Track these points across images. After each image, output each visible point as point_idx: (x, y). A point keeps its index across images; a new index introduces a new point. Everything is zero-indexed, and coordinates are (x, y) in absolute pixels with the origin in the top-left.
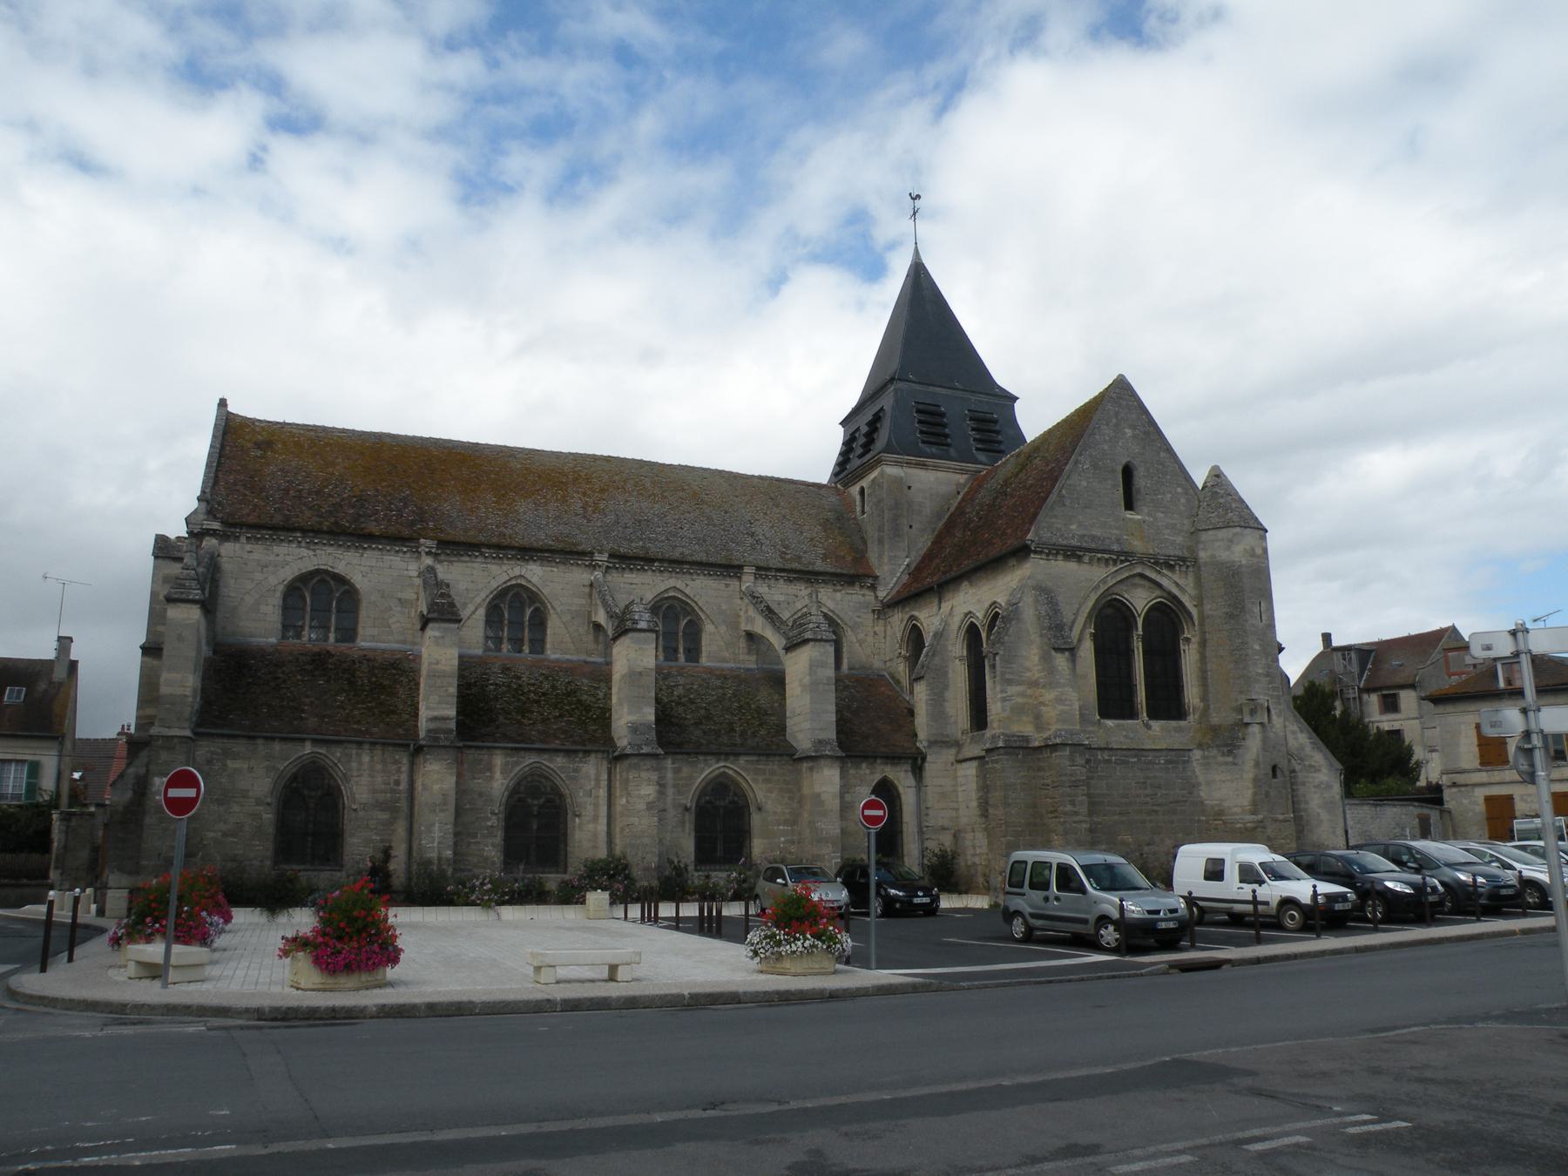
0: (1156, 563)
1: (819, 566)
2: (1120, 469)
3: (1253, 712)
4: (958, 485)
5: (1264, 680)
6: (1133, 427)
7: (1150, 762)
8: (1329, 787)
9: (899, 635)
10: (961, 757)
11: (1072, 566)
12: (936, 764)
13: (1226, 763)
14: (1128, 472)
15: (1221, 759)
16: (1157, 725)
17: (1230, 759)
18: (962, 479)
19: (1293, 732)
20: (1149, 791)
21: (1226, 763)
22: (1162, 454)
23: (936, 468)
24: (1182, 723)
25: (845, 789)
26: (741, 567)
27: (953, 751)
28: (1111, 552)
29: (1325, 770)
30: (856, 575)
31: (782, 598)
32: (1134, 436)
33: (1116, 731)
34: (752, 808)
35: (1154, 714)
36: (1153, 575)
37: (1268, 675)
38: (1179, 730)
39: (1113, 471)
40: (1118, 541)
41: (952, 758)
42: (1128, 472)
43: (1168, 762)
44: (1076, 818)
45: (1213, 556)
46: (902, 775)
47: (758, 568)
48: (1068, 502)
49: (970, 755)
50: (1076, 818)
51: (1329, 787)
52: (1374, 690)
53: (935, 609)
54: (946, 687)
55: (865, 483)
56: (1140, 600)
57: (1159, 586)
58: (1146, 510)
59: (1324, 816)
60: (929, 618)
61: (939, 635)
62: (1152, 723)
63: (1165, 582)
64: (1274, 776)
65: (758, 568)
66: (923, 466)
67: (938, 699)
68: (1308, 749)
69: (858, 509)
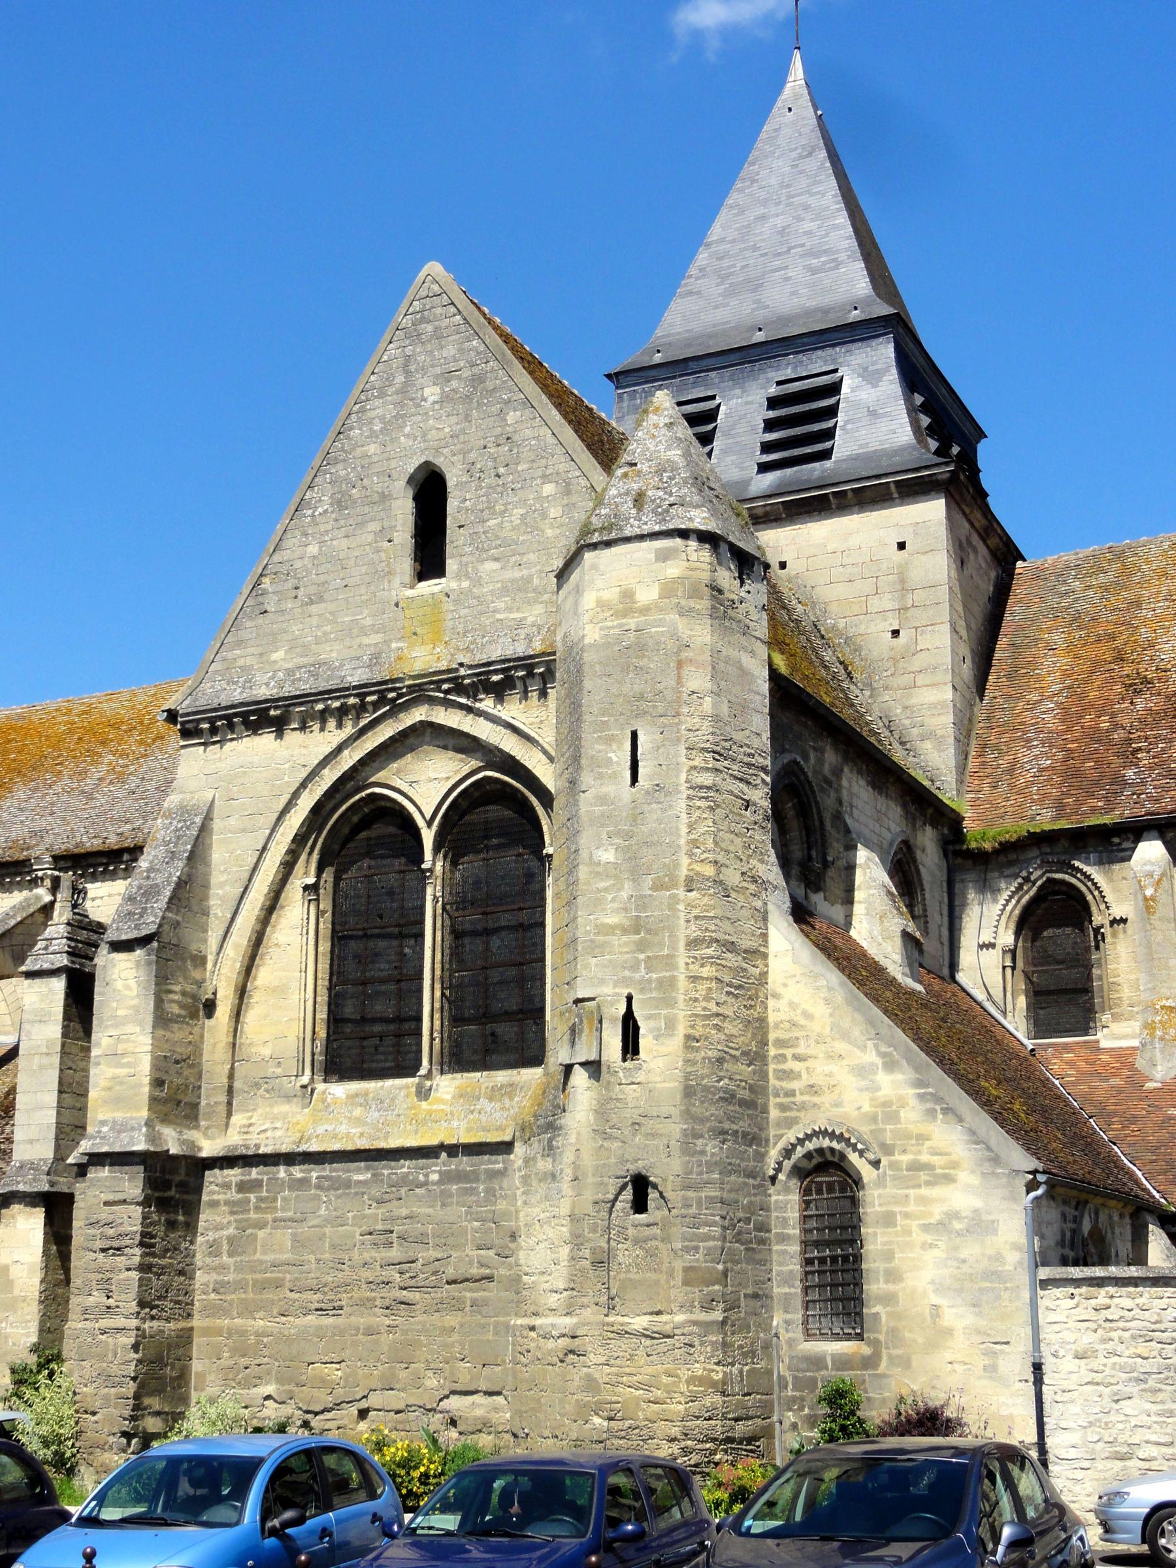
11: (266, 740)
14: (430, 491)
19: (862, 1071)
20: (395, 1253)
29: (965, 1177)
32: (445, 399)
33: (356, 1112)
35: (460, 1057)
42: (430, 491)
43: (446, 1178)
44: (104, 1323)
50: (104, 1323)
51: (979, 1226)
56: (426, 785)
58: (451, 565)
59: (957, 1317)
64: (640, 1205)
68: (912, 1115)
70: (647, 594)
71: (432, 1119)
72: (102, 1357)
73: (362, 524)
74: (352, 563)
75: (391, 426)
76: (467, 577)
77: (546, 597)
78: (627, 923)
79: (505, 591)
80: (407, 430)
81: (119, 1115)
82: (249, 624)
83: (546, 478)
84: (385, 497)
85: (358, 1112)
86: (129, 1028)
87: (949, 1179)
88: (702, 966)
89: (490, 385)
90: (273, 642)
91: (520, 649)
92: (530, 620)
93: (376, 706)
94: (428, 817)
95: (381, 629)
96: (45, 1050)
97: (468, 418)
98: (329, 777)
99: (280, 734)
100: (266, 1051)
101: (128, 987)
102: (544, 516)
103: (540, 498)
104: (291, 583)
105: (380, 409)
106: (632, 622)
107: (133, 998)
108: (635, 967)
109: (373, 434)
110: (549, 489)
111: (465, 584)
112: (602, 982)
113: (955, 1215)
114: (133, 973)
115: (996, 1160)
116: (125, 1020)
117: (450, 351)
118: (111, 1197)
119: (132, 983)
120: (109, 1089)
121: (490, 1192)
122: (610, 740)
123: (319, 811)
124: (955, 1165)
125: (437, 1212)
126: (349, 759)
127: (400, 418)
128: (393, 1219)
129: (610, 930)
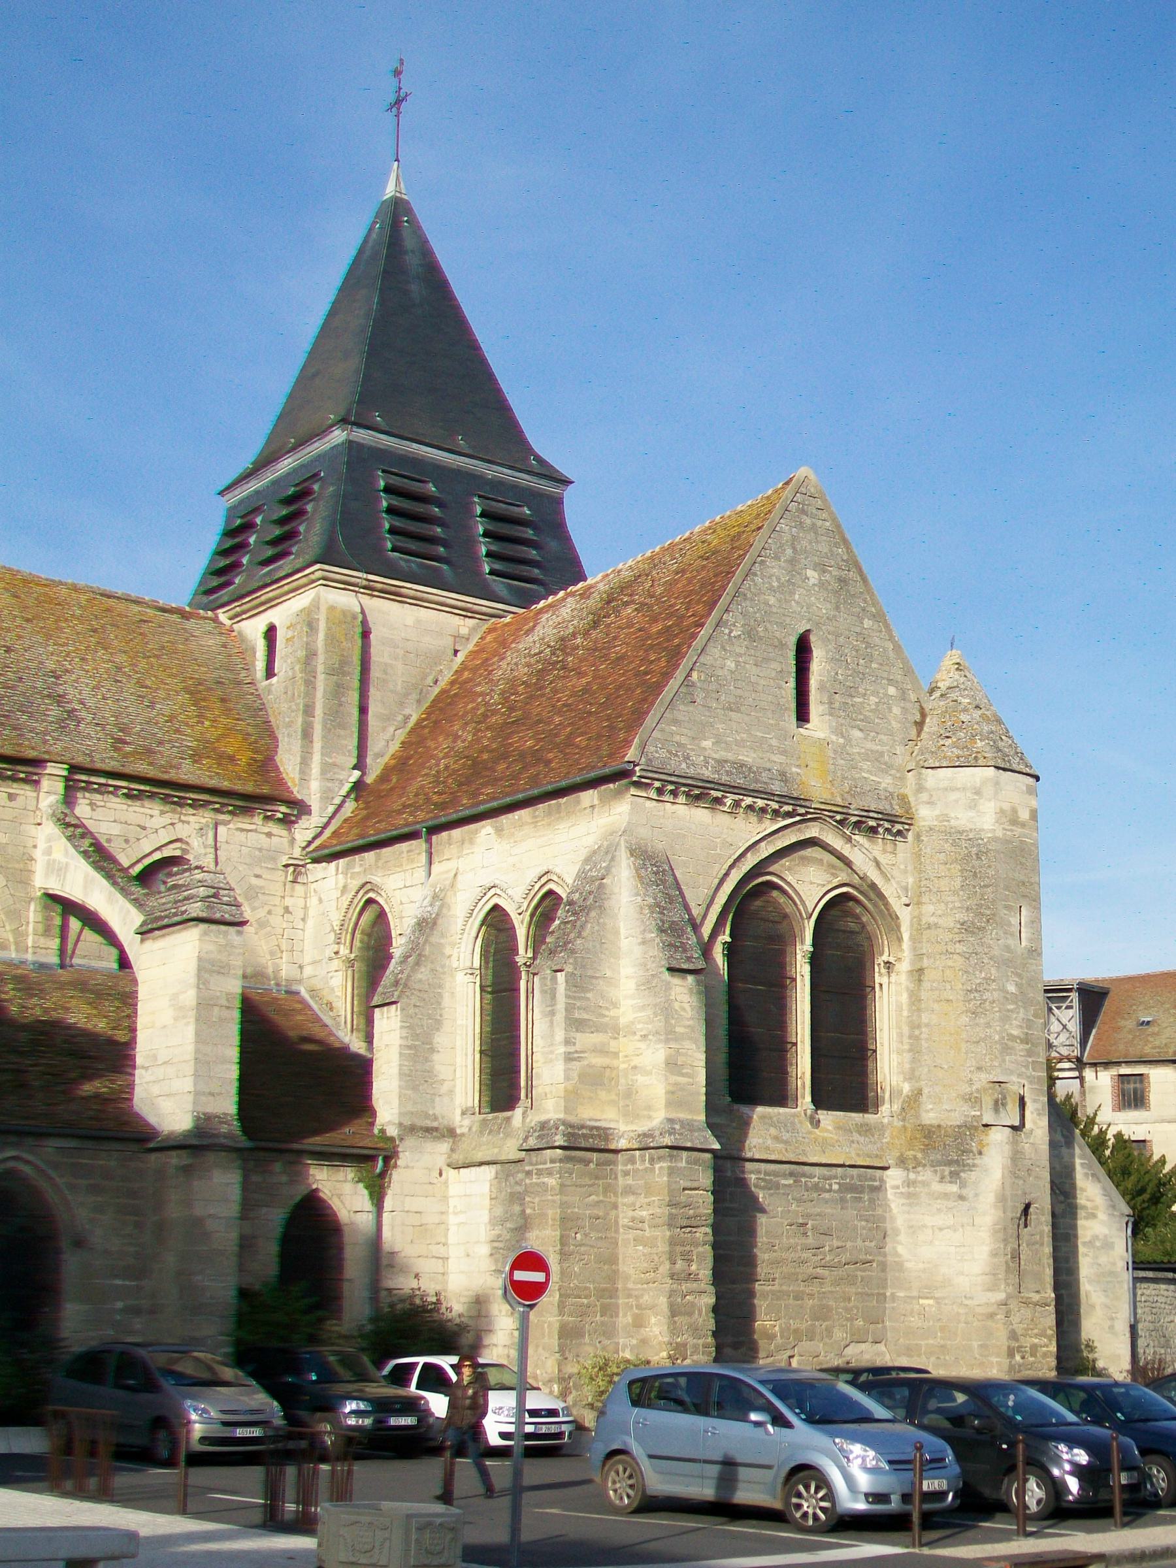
1: (187, 772)
2: (792, 641)
3: (998, 1105)
4: (457, 637)
5: (1020, 1047)
6: (821, 568)
7: (816, 1188)
8: (1108, 1245)
9: (336, 918)
10: (459, 1157)
11: (700, 815)
12: (414, 1167)
13: (946, 1196)
15: (937, 1187)
16: (829, 1119)
17: (954, 1188)
18: (465, 626)
20: (810, 1241)
21: (946, 1196)
22: (867, 623)
23: (418, 601)
24: (869, 1117)
25: (248, 1207)
26: (38, 763)
27: (444, 1147)
28: (769, 795)
29: (1102, 1216)
30: (260, 795)
31: (115, 829)
32: (822, 584)
34: (65, 1243)
35: (821, 1100)
36: (836, 842)
37: (1026, 1040)
38: (865, 1130)
39: (783, 645)
40: (784, 776)
41: (441, 1161)
46: (348, 1188)
47: (74, 768)
48: (700, 696)
49: (479, 1156)
51: (1108, 1245)
52: (1107, 1065)
53: (421, 873)
54: (438, 1024)
55: (281, 615)
57: (848, 863)
60: (401, 882)
61: (426, 925)
62: (823, 1115)
65: (74, 768)
66: (395, 595)
67: (420, 1048)
69: (260, 665)
70: (1024, 815)
71: (824, 1145)
72: (690, 1314)
73: (767, 660)
74: (760, 688)
75: (787, 588)
76: (843, 737)
77: (893, 772)
78: (1022, 1036)
80: (797, 597)
82: (682, 707)
83: (891, 682)
85: (773, 1131)
87: (1094, 1216)
92: (883, 785)
93: (789, 815)
94: (810, 911)
96: (225, 1003)
99: (760, 820)
101: (684, 1009)
103: (886, 695)
105: (776, 570)
106: (1018, 830)
107: (688, 1019)
108: (1026, 1067)
109: (771, 588)
110: (892, 691)
111: (841, 741)
112: (1012, 1072)
113: (1096, 1237)
114: (686, 998)
115: (1113, 1207)
118: (689, 1184)
119: (687, 1006)
120: (673, 1093)
121: (872, 1201)
124: (1096, 1208)
126: (766, 850)
128: (809, 1216)
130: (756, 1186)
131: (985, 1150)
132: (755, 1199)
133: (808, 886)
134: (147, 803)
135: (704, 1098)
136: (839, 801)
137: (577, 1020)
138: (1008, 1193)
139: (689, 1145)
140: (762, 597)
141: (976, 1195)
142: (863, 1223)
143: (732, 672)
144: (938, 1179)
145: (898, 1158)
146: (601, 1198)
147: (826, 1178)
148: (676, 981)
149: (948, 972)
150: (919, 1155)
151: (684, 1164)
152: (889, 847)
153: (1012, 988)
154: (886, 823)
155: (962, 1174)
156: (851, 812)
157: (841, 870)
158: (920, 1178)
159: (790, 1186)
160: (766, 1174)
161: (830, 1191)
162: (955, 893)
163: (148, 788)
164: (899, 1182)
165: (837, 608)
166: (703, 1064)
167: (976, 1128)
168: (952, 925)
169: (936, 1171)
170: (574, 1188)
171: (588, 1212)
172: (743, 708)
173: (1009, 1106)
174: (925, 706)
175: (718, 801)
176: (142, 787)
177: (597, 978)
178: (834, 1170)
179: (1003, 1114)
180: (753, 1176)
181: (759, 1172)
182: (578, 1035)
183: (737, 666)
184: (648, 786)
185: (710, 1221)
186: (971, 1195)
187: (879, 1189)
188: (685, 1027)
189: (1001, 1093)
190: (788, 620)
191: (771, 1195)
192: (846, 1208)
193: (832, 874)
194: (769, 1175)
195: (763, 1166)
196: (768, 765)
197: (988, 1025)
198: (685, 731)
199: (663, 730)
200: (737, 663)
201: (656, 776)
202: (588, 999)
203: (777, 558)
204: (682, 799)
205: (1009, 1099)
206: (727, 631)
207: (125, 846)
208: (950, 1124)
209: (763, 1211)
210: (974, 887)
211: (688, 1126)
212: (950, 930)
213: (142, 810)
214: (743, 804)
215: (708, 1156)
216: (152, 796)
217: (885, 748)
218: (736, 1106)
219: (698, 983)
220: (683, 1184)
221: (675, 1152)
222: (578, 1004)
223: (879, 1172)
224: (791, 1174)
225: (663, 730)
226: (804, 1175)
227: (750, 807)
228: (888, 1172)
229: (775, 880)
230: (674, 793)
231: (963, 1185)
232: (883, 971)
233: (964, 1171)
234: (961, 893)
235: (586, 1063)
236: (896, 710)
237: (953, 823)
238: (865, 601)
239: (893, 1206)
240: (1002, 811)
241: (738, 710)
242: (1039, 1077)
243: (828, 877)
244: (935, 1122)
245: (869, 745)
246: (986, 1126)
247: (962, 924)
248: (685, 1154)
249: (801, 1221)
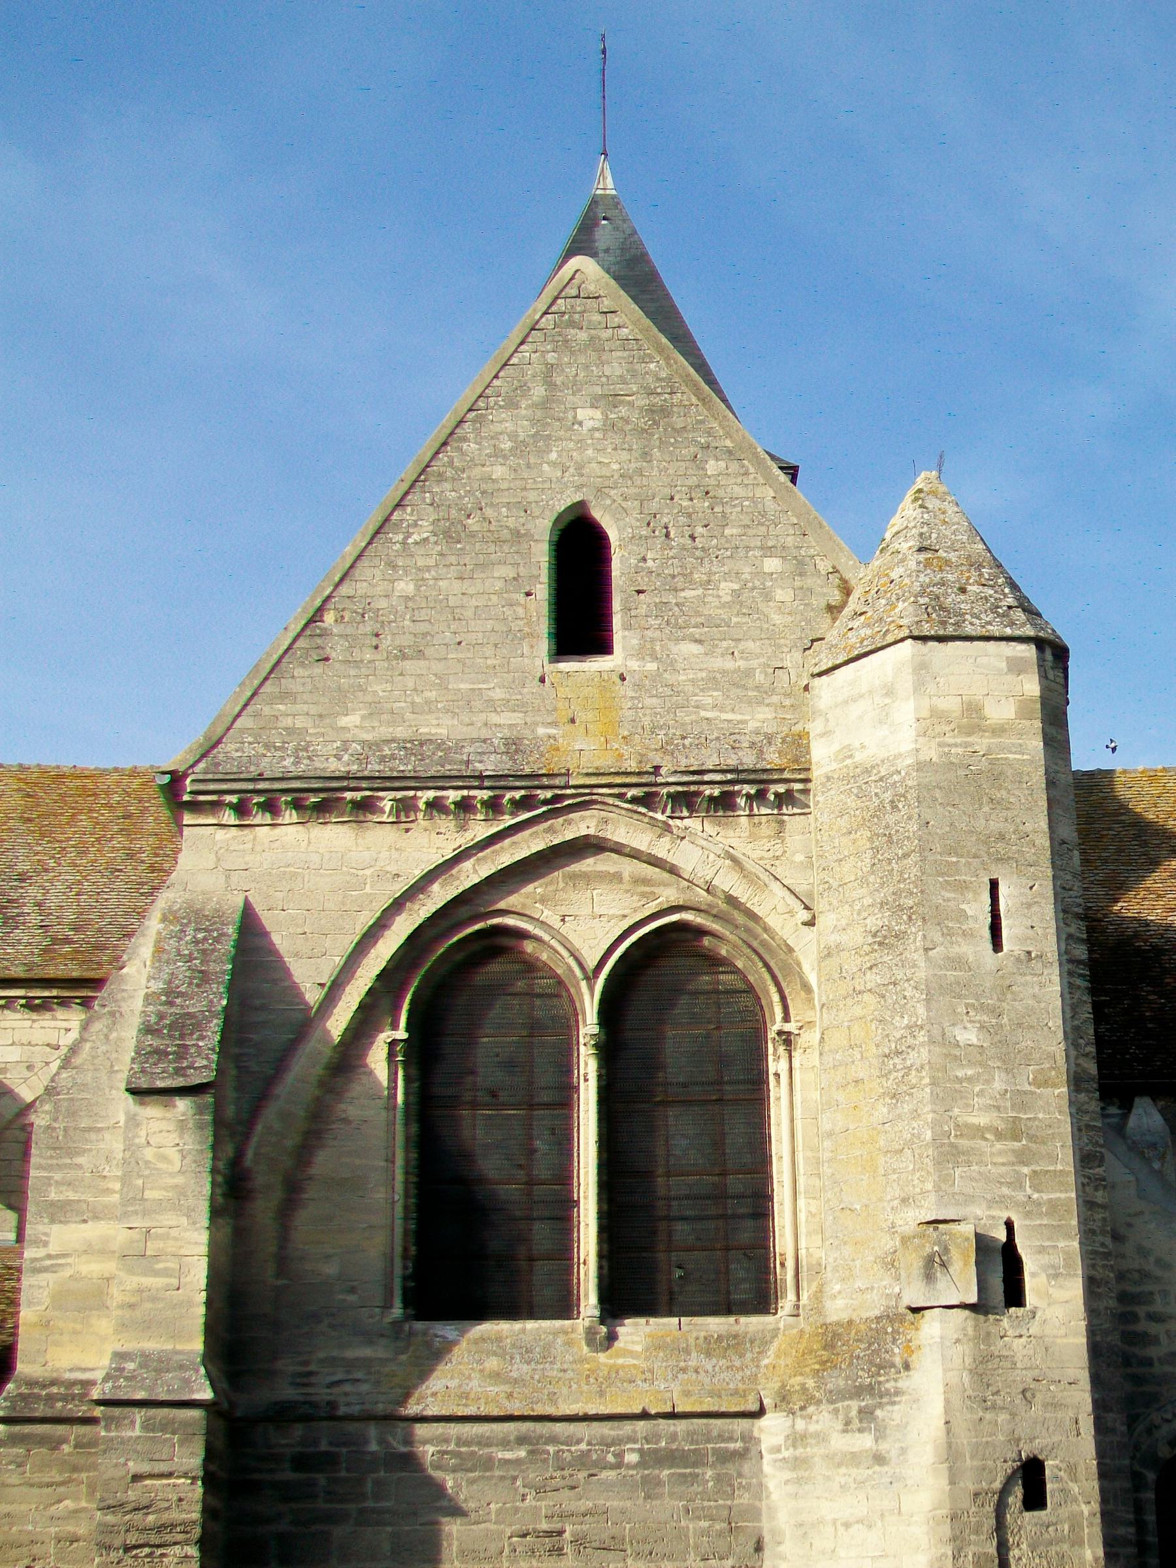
0: (647, 801)
5: (997, 1151)
6: (613, 400)
7: (582, 1460)
11: (333, 837)
13: (854, 1459)
15: (840, 1442)
17: (865, 1441)
22: (712, 467)
32: (609, 427)
37: (1014, 1131)
43: (652, 1458)
45: (847, 753)
48: (337, 650)
63: (686, 857)
74: (469, 613)
76: (655, 658)
77: (775, 699)
78: (1001, 1126)
79: (713, 681)
80: (553, 456)
81: (151, 1345)
82: (299, 672)
84: (518, 536)
85: (493, 1363)
86: (169, 1219)
88: (1096, 1189)
89: (679, 423)
90: (342, 700)
91: (749, 760)
92: (752, 725)
94: (591, 962)
95: (520, 707)
97: (646, 455)
98: (440, 895)
100: (331, 1269)
101: (164, 1158)
102: (768, 597)
103: (759, 574)
104: (368, 628)
106: (981, 743)
107: (172, 1175)
108: (1017, 1184)
109: (498, 454)
110: (772, 564)
111: (652, 666)
112: (969, 1199)
114: (174, 1138)
116: (160, 1206)
117: (615, 369)
118: (145, 1468)
120: (132, 1306)
122: (962, 887)
123: (417, 942)
125: (635, 1504)
126: (472, 874)
127: (540, 440)
129: (979, 1132)
130: (438, 1467)
131: (914, 1360)
132: (439, 1490)
133: (581, 926)
134: (61, 1013)
135: (202, 1310)
136: (632, 765)
137: (53, 1204)
138: (964, 1440)
139: (140, 1395)
140: (477, 472)
141: (903, 1451)
142: (704, 1524)
143: (407, 598)
144: (839, 1426)
145: (778, 1393)
146: (84, 1504)
147: (607, 1443)
148: (152, 1112)
149: (857, 1029)
150: (811, 1383)
151: (137, 1432)
152: (767, 829)
153: (968, 1036)
154: (763, 788)
155: (878, 1413)
156: (660, 780)
157: (666, 885)
158: (813, 1428)
159: (518, 1462)
160: (460, 1442)
161: (619, 1465)
162: (863, 881)
163: (54, 993)
164: (779, 1440)
165: (646, 455)
166: (204, 1249)
167: (901, 1319)
168: (860, 940)
169: (836, 1411)
170: (24, 1489)
171: (53, 1530)
172: (429, 652)
173: (956, 1267)
174: (848, 576)
175: (366, 806)
176: (46, 994)
177: (100, 1130)
178: (628, 1427)
179: (942, 1282)
180: (431, 1449)
181: (447, 1441)
182: (56, 1228)
183: (418, 588)
184: (216, 806)
185: (197, 1532)
186: (894, 1454)
187: (747, 1451)
188: (165, 1189)
189: (939, 1243)
190: (532, 496)
191: (472, 1482)
192: (660, 1496)
193: (643, 895)
194: (467, 1443)
195: (454, 1429)
196: (484, 733)
197: (916, 1114)
198: (305, 708)
199: (257, 715)
200: (420, 582)
201: (224, 787)
202: (80, 1166)
203: (512, 404)
204: (290, 816)
205: (955, 1253)
206: (400, 537)
207: (28, 1074)
208: (865, 1315)
209: (457, 1511)
210: (889, 861)
211: (159, 1364)
212: (857, 950)
213: (53, 1024)
214: (421, 805)
215: (196, 1414)
216: (64, 1002)
217: (754, 663)
218: (419, 1325)
219: (200, 1110)
220: (134, 1467)
221: (117, 1411)
222: (58, 1176)
223: (744, 1423)
224: (522, 1440)
225: (257, 715)
226: (553, 1440)
227: (435, 806)
228: (764, 1422)
229: (510, 921)
230: (270, 807)
231: (880, 1435)
232: (781, 1049)
233: (880, 1405)
234: (872, 879)
235: (67, 1273)
236: (782, 594)
237: (859, 757)
238: (709, 432)
239: (771, 1484)
240: (937, 715)
241: (420, 654)
242: (1053, 1206)
243: (635, 902)
244: (844, 1316)
245: (718, 663)
246: (916, 1310)
247: (875, 936)
248: (139, 1415)
249: (544, 1526)
